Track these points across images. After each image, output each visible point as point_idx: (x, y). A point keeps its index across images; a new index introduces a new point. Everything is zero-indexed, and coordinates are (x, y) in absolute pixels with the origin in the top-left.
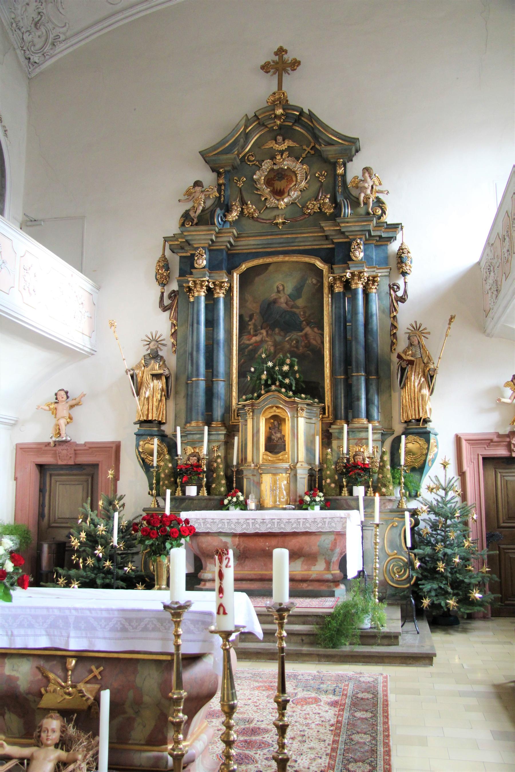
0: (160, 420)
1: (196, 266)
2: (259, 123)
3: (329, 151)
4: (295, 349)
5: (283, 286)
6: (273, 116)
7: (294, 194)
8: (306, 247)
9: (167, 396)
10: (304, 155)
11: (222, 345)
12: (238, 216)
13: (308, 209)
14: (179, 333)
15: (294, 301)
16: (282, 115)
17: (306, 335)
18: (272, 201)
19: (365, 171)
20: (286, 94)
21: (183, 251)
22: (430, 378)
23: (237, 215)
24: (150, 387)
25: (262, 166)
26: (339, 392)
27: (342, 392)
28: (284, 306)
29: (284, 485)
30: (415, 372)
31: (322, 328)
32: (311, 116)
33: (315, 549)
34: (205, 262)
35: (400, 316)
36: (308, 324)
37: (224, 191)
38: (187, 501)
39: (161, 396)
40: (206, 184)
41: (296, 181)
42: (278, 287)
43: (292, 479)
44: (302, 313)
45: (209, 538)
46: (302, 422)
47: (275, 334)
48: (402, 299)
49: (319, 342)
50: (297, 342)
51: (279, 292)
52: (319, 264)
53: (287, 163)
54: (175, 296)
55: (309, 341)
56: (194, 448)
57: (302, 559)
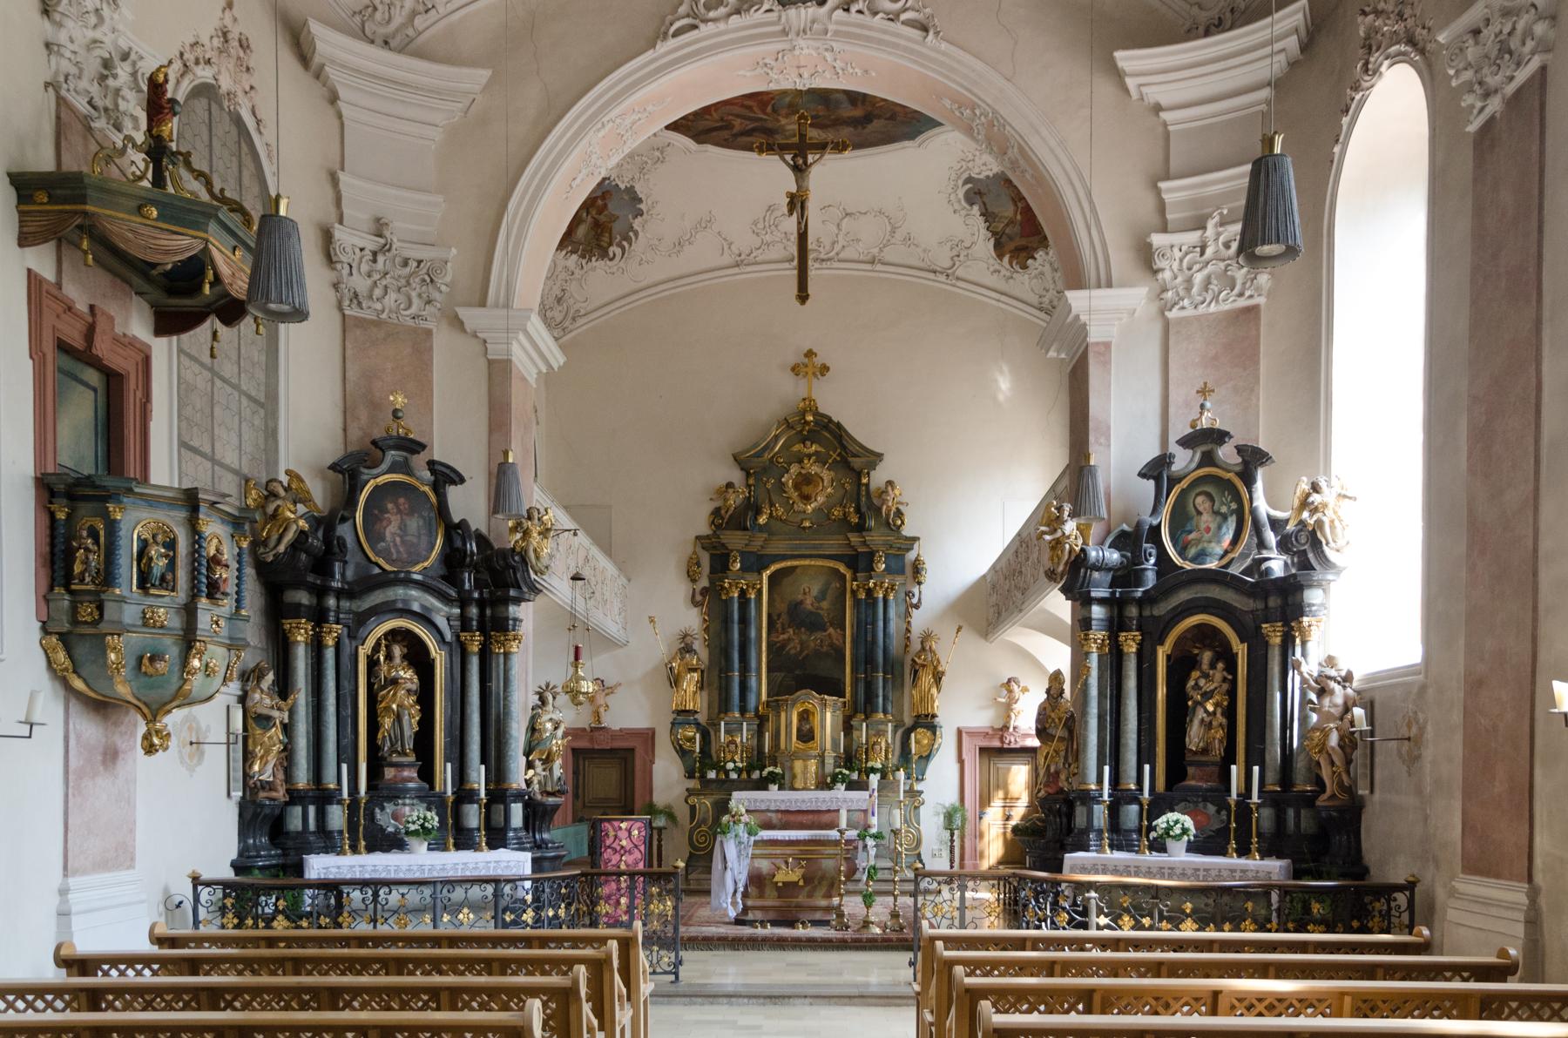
3: (856, 463)
7: (821, 499)
18: (800, 506)
32: (839, 425)
52: (842, 569)
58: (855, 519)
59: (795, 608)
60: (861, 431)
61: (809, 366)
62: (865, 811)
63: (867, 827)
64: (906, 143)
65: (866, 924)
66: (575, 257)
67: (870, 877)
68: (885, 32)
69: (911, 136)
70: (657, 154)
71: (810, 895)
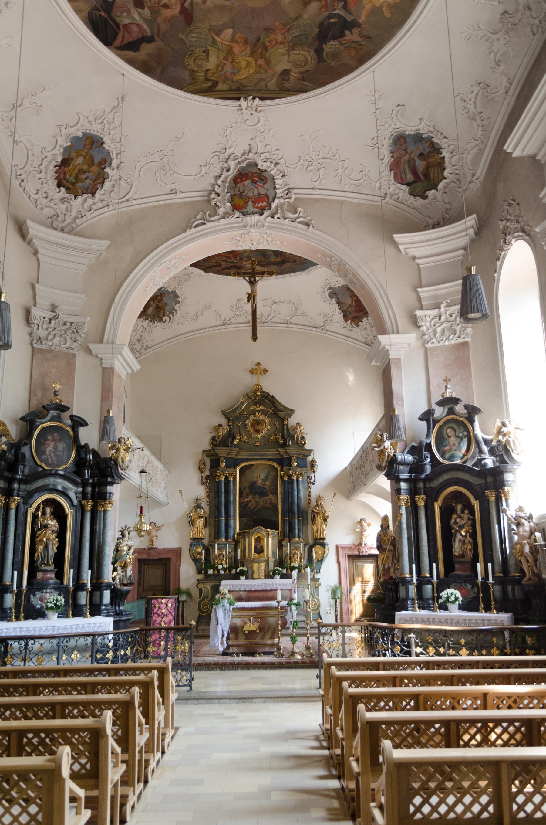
3: (281, 414)
7: (265, 432)
9: (205, 526)
18: (254, 435)
22: (325, 519)
32: (273, 397)
36: (271, 493)
40: (223, 425)
46: (270, 539)
48: (313, 483)
52: (276, 465)
53: (261, 417)
58: (281, 441)
59: (253, 485)
61: (258, 370)
62: (291, 590)
63: (291, 599)
64: (301, 273)
65: (293, 653)
66: (147, 321)
67: (294, 627)
68: (290, 226)
69: (303, 270)
70: (187, 277)
71: (263, 638)
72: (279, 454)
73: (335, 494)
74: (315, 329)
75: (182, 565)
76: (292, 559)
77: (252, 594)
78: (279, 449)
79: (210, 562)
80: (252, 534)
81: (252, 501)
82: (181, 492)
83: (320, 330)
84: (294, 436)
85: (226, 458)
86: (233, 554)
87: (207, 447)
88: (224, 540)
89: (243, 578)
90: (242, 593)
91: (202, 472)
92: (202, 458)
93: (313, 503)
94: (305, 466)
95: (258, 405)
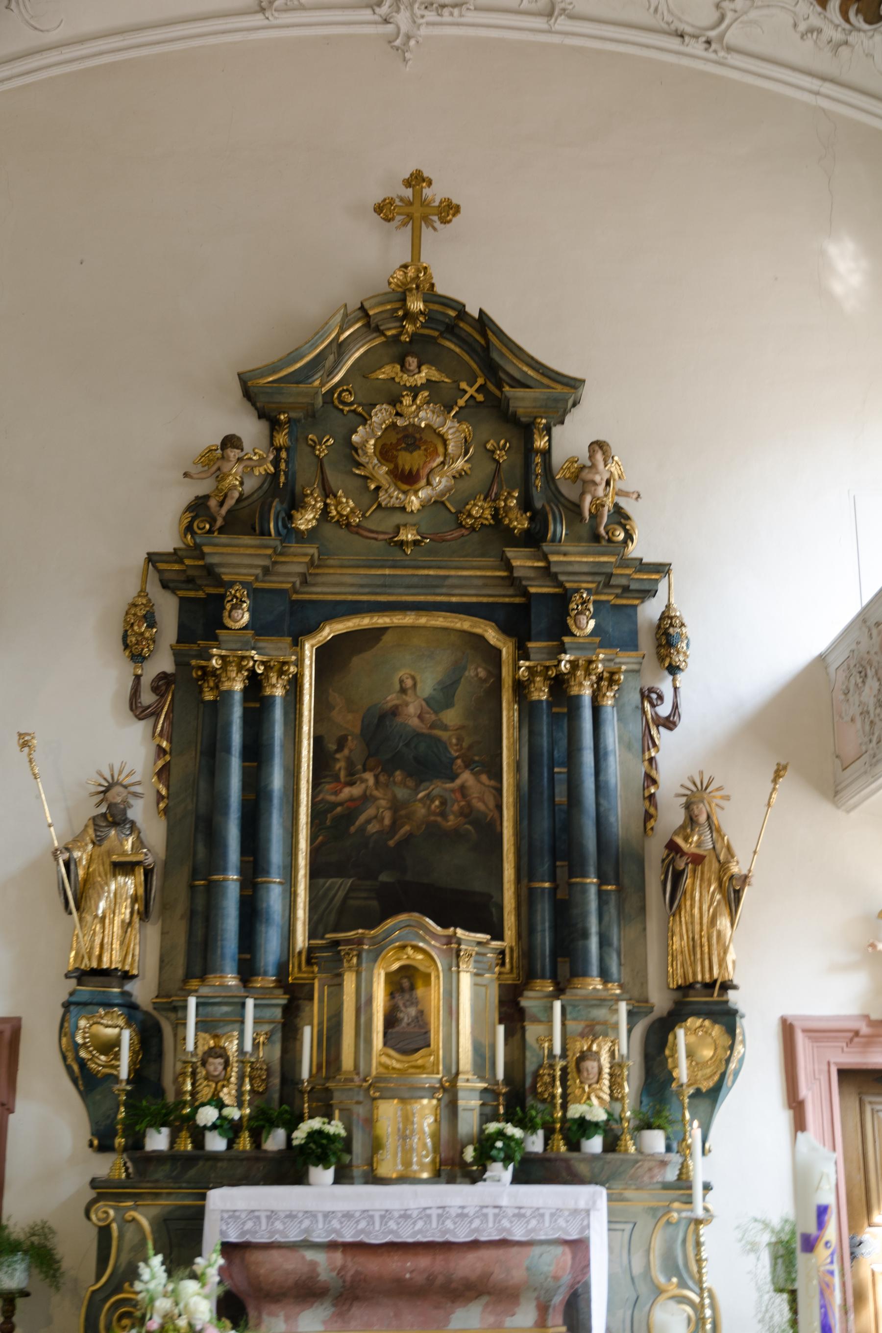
0: (127, 968)
1: (228, 622)
2: (367, 325)
3: (522, 400)
4: (439, 819)
5: (413, 678)
6: (400, 313)
7: (441, 482)
8: (466, 599)
9: (145, 915)
10: (461, 402)
11: (276, 801)
12: (317, 520)
13: (470, 515)
14: (174, 770)
15: (436, 713)
16: (421, 312)
17: (463, 788)
18: (392, 495)
19: (597, 448)
20: (429, 271)
21: (191, 586)
22: (732, 893)
23: (314, 518)
24: (109, 892)
25: (371, 417)
26: (539, 918)
27: (547, 917)
28: (414, 722)
29: (429, 1125)
30: (702, 880)
31: (498, 776)
32: (484, 322)
33: (518, 1275)
34: (247, 617)
35: (661, 757)
36: (469, 764)
37: (287, 462)
38: (201, 1163)
39: (132, 913)
40: (247, 445)
41: (445, 455)
42: (401, 681)
43: (445, 1113)
44: (454, 741)
45: (275, 1254)
46: (466, 981)
47: (395, 783)
48: (669, 723)
49: (491, 804)
50: (444, 803)
51: (403, 691)
52: (492, 635)
54: (168, 685)
55: (469, 804)
56: (216, 1037)
57: (485, 1299)
58: (520, 523)
59: (380, 726)
60: (533, 329)
61: (416, 207)
72: (512, 581)
73: (778, 774)
74: (674, 43)
75: (20, 1105)
76: (574, 1082)
77: (373, 1266)
78: (510, 552)
79: (160, 1092)
80: (376, 955)
81: (377, 799)
82: (25, 743)
83: (697, 48)
84: (576, 509)
85: (255, 594)
86: (277, 1052)
87: (166, 538)
88: (232, 980)
89: (323, 1175)
90: (320, 1258)
91: (138, 658)
92: (143, 593)
93: (671, 816)
94: (631, 643)
95: (412, 362)
